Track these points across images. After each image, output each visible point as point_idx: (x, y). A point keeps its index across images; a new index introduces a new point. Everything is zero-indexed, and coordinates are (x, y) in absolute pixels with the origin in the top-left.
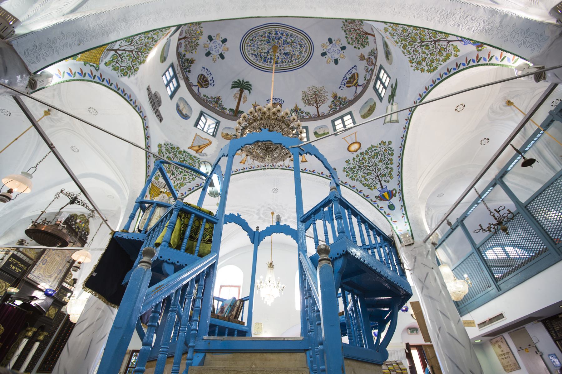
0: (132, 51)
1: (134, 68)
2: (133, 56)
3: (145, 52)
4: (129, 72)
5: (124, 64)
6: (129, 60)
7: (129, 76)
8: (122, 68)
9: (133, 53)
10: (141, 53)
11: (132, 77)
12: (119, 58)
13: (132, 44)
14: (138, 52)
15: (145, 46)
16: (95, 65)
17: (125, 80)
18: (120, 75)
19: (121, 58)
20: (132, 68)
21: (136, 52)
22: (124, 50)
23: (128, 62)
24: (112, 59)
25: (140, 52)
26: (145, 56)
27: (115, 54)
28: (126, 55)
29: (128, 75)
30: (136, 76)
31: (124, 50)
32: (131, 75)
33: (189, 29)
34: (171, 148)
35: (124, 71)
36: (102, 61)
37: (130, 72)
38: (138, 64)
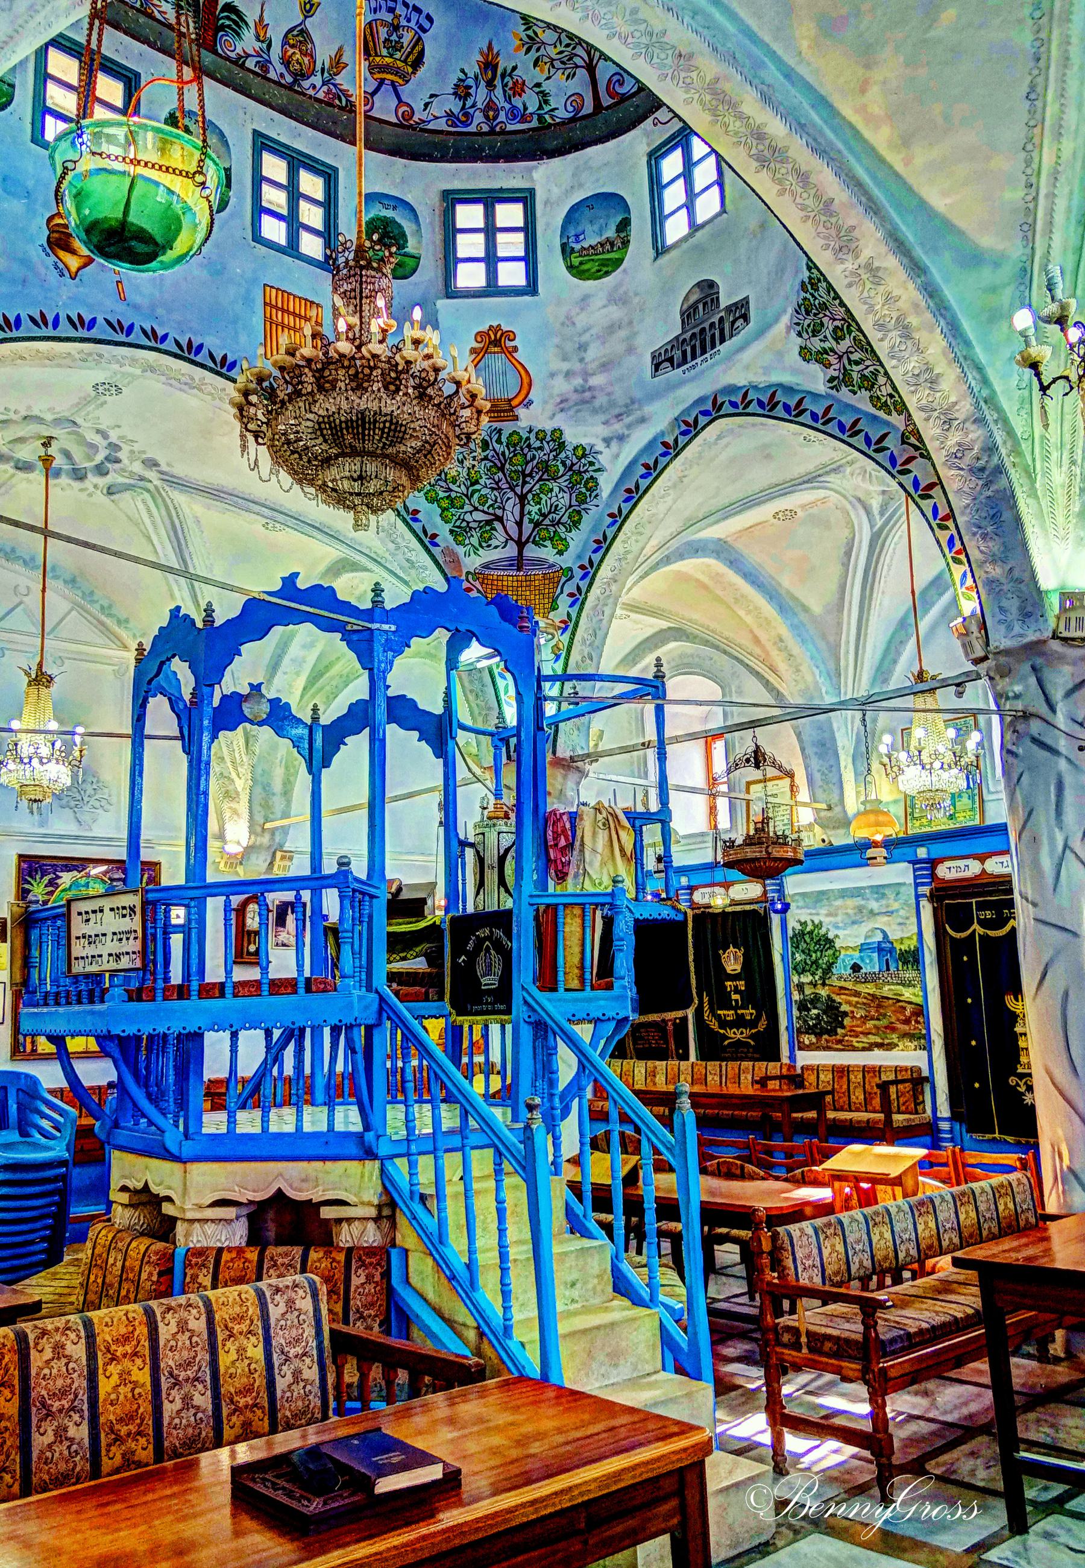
0: (522, 498)
1: (575, 460)
2: (537, 486)
3: (526, 450)
4: (586, 476)
5: (564, 500)
6: (552, 490)
7: (599, 470)
8: (574, 502)
9: (530, 491)
10: (527, 463)
11: (604, 459)
12: (547, 522)
13: (499, 512)
14: (525, 476)
15: (502, 469)
16: (564, 579)
17: (606, 484)
18: (595, 502)
19: (545, 516)
20: (576, 468)
21: (525, 483)
22: (519, 524)
23: (556, 489)
24: (548, 543)
25: (523, 471)
26: (538, 444)
27: (534, 542)
28: (535, 509)
29: (595, 475)
30: (600, 446)
31: (519, 524)
32: (597, 466)
33: (557, 64)
34: (808, 313)
35: (584, 490)
36: (552, 566)
37: (586, 471)
38: (563, 455)
